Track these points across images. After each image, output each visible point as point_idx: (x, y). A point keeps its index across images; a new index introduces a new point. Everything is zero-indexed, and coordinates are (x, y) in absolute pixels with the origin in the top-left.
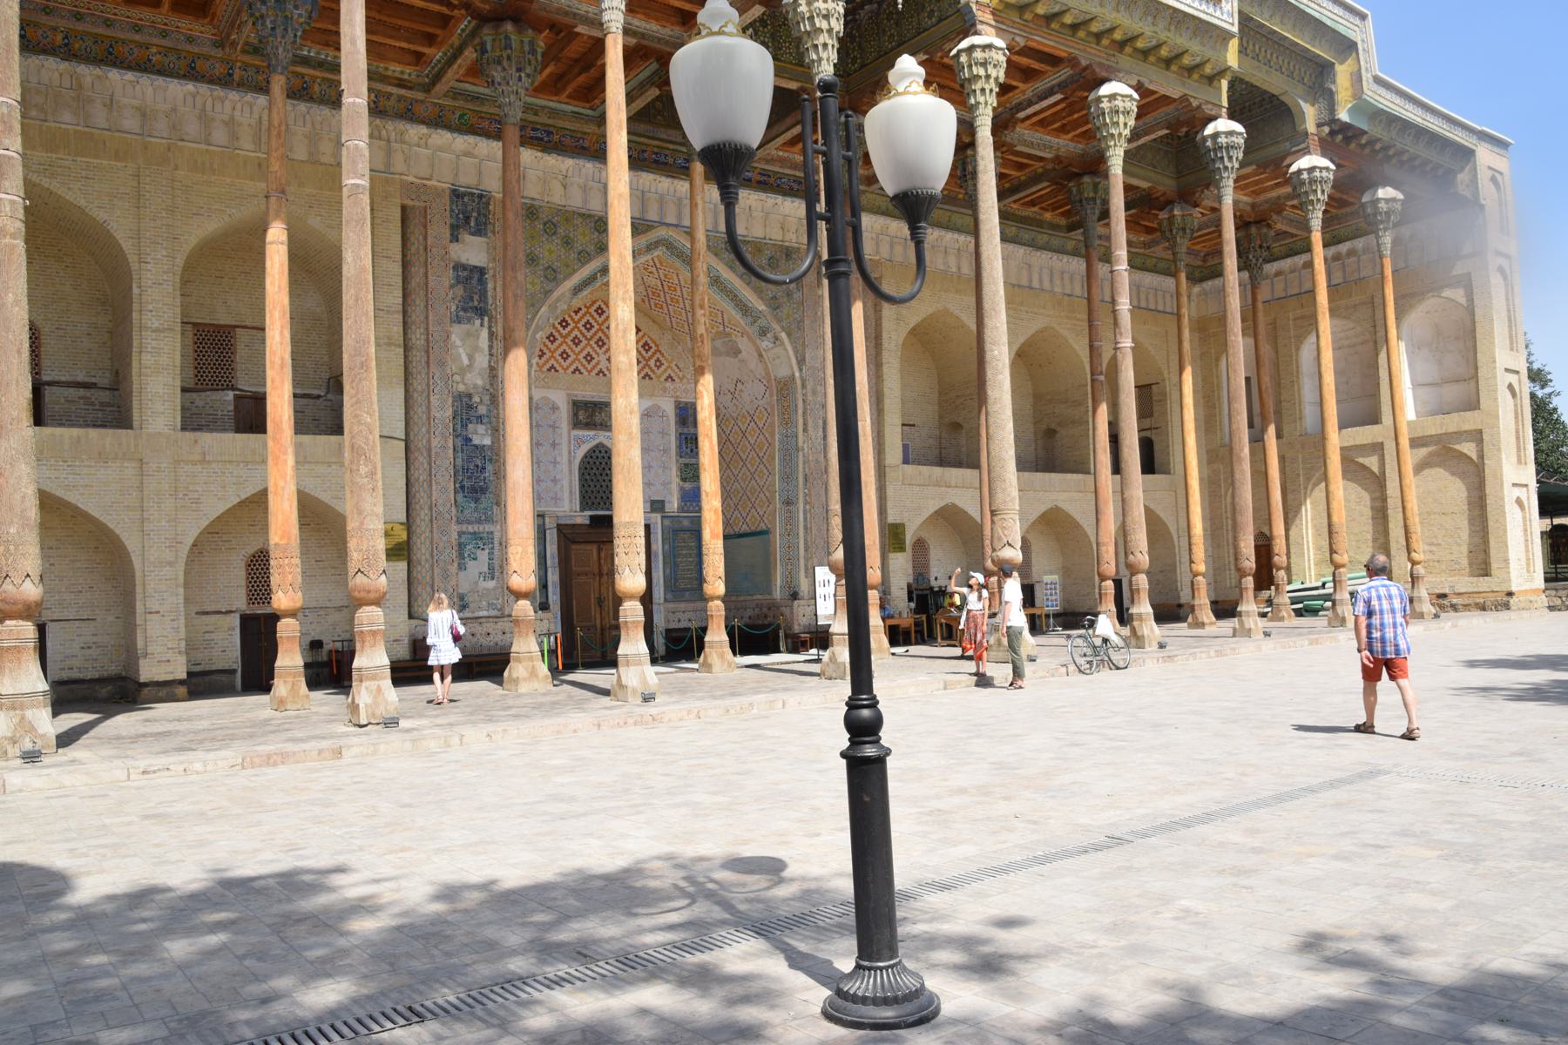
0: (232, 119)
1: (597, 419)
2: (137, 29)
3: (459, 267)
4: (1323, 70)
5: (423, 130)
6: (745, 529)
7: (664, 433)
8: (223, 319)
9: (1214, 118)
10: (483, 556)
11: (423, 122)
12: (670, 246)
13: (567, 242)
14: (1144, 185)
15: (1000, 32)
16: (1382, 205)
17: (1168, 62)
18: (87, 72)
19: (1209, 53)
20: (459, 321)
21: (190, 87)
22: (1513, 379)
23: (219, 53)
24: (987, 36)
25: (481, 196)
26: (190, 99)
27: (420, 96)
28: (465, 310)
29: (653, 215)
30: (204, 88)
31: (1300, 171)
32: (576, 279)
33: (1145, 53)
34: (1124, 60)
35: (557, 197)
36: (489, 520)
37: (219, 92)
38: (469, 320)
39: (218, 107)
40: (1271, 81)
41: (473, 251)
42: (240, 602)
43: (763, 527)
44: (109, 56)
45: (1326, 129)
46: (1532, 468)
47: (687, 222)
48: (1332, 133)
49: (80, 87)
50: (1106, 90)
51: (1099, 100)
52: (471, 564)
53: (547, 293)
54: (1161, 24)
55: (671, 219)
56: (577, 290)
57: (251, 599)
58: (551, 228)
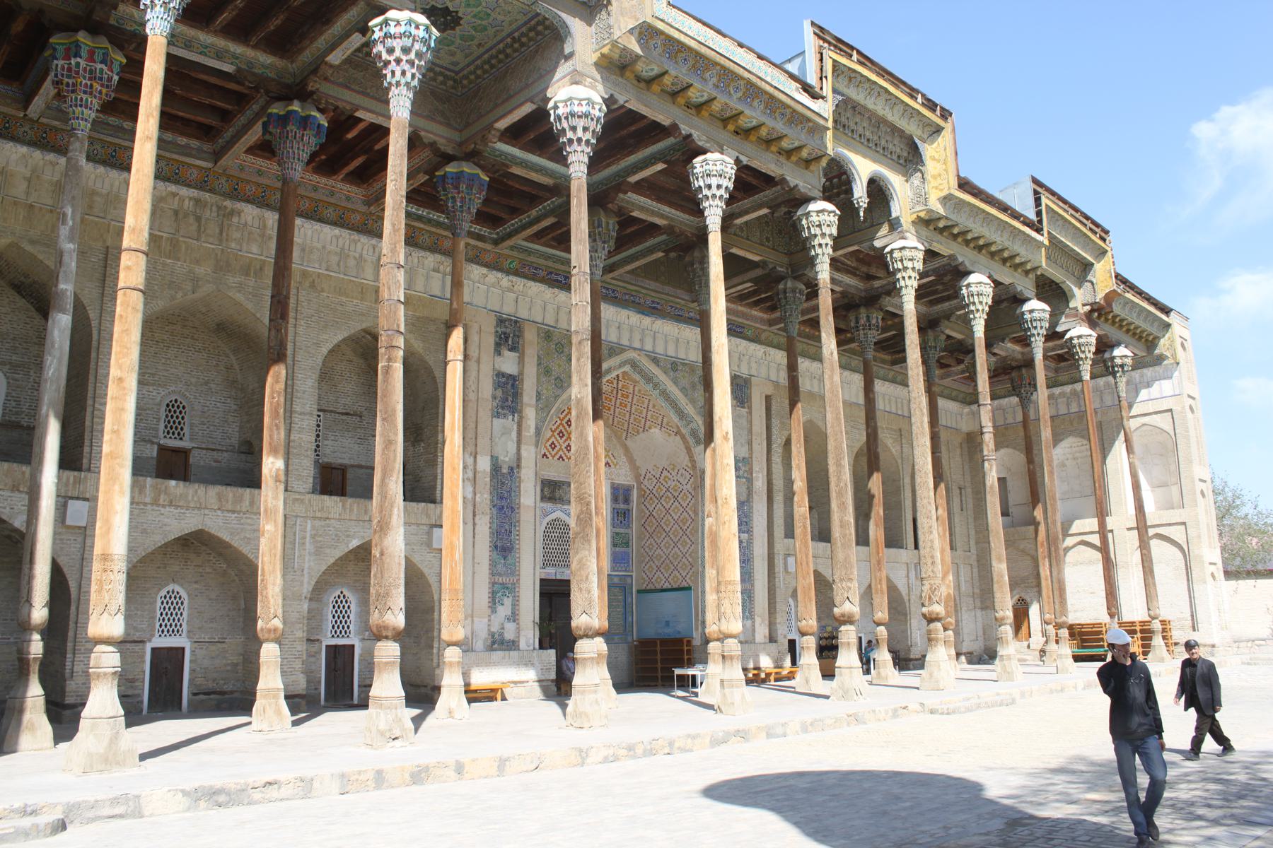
0: (361, 256)
1: (557, 495)
2: (315, 189)
3: (500, 374)
4: (1087, 267)
5: (484, 270)
6: (667, 586)
9: (1029, 299)
10: (508, 602)
11: (486, 266)
12: (634, 364)
14: (959, 336)
15: (919, 238)
16: (1118, 361)
17: (1004, 261)
19: (1030, 257)
20: (498, 415)
21: (337, 231)
22: (1202, 486)
23: (363, 209)
24: (912, 241)
25: (516, 322)
26: (334, 240)
27: (488, 246)
28: (503, 408)
29: (625, 342)
30: (345, 233)
31: (1071, 339)
33: (993, 255)
34: (983, 258)
36: (512, 574)
37: (355, 236)
38: (505, 416)
39: (352, 248)
40: (1057, 274)
43: (684, 584)
45: (1088, 308)
46: (1218, 551)
47: (649, 347)
48: (1092, 311)
49: (265, 226)
50: (973, 278)
51: (968, 285)
52: (500, 608)
53: (557, 397)
54: (1006, 235)
55: (637, 345)
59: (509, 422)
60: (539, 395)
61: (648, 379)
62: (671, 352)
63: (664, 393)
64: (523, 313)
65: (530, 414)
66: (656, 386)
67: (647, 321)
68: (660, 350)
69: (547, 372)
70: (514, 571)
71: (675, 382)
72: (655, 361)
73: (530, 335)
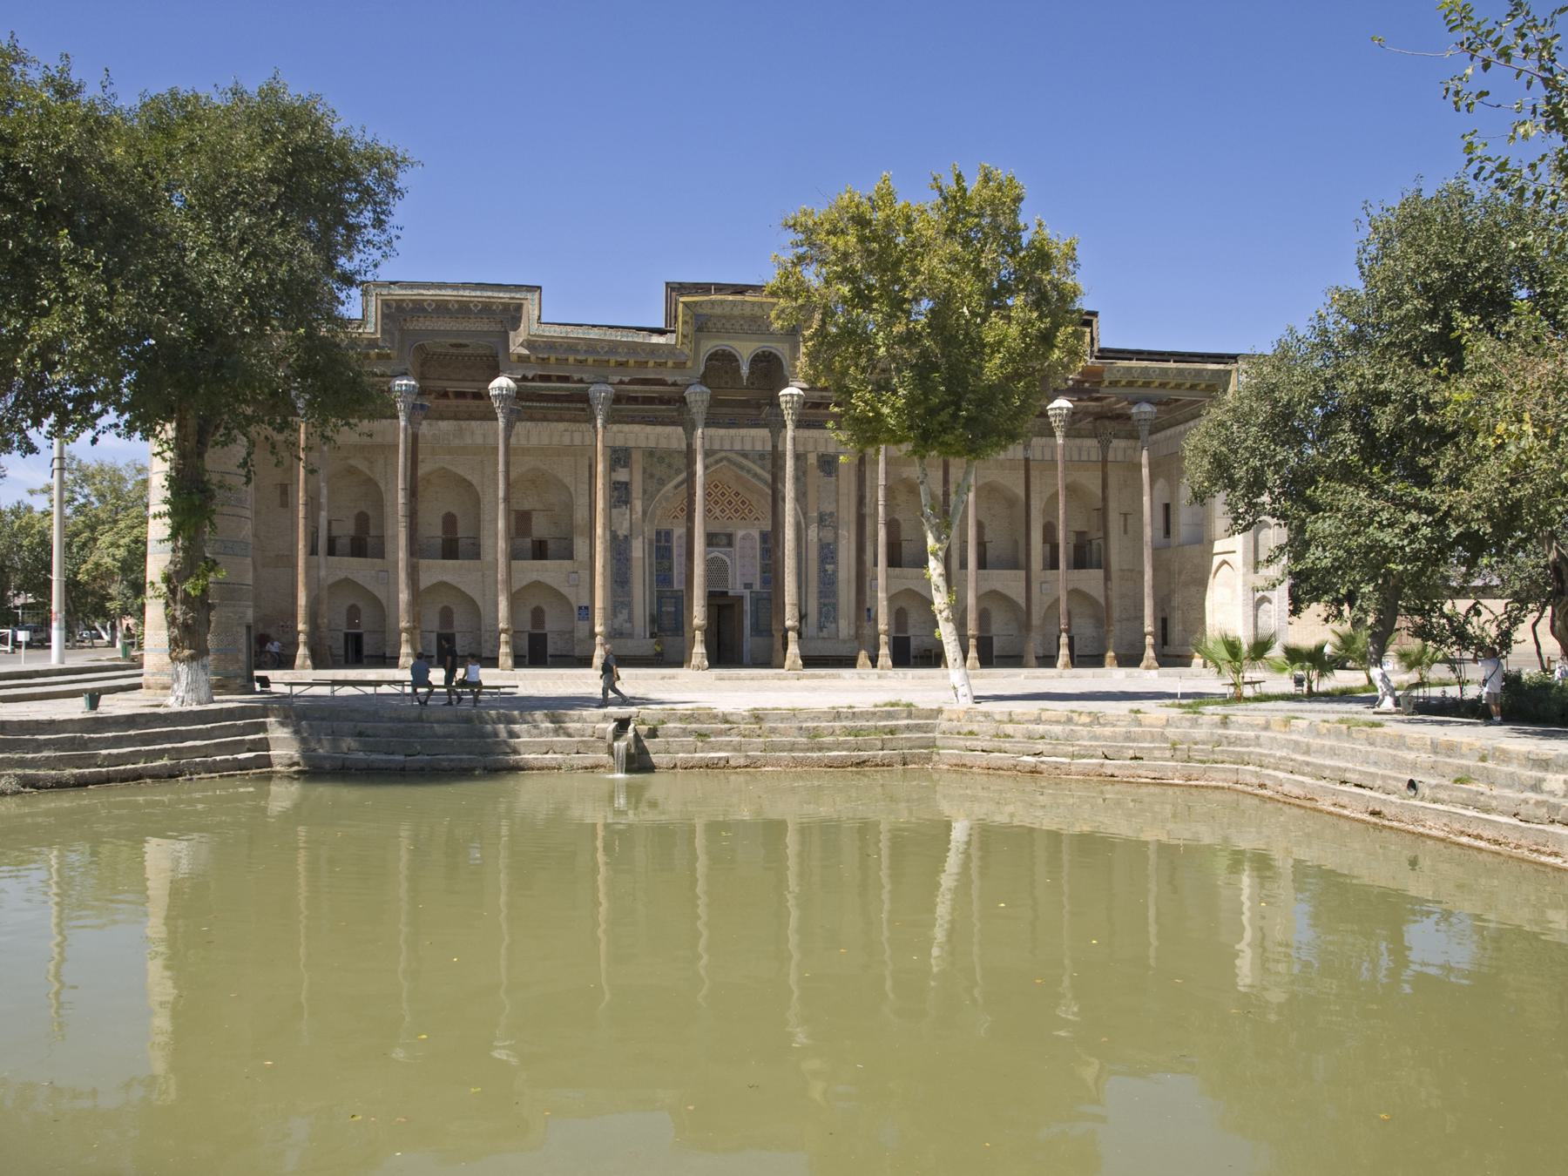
7: (753, 548)
8: (526, 506)
10: (625, 612)
12: (729, 460)
13: (670, 466)
18: (464, 424)
29: (716, 447)
32: (675, 482)
35: (663, 444)
41: (622, 475)
42: (528, 628)
44: (471, 417)
47: (737, 447)
55: (727, 447)
56: (676, 487)
57: (533, 627)
58: (661, 460)
59: (625, 510)
60: (645, 492)
61: (742, 467)
62: (759, 447)
63: (755, 475)
64: (631, 444)
65: (638, 505)
66: (749, 471)
67: (732, 432)
68: (748, 447)
69: (652, 476)
70: (629, 594)
71: (763, 467)
72: (745, 455)
73: (637, 457)
